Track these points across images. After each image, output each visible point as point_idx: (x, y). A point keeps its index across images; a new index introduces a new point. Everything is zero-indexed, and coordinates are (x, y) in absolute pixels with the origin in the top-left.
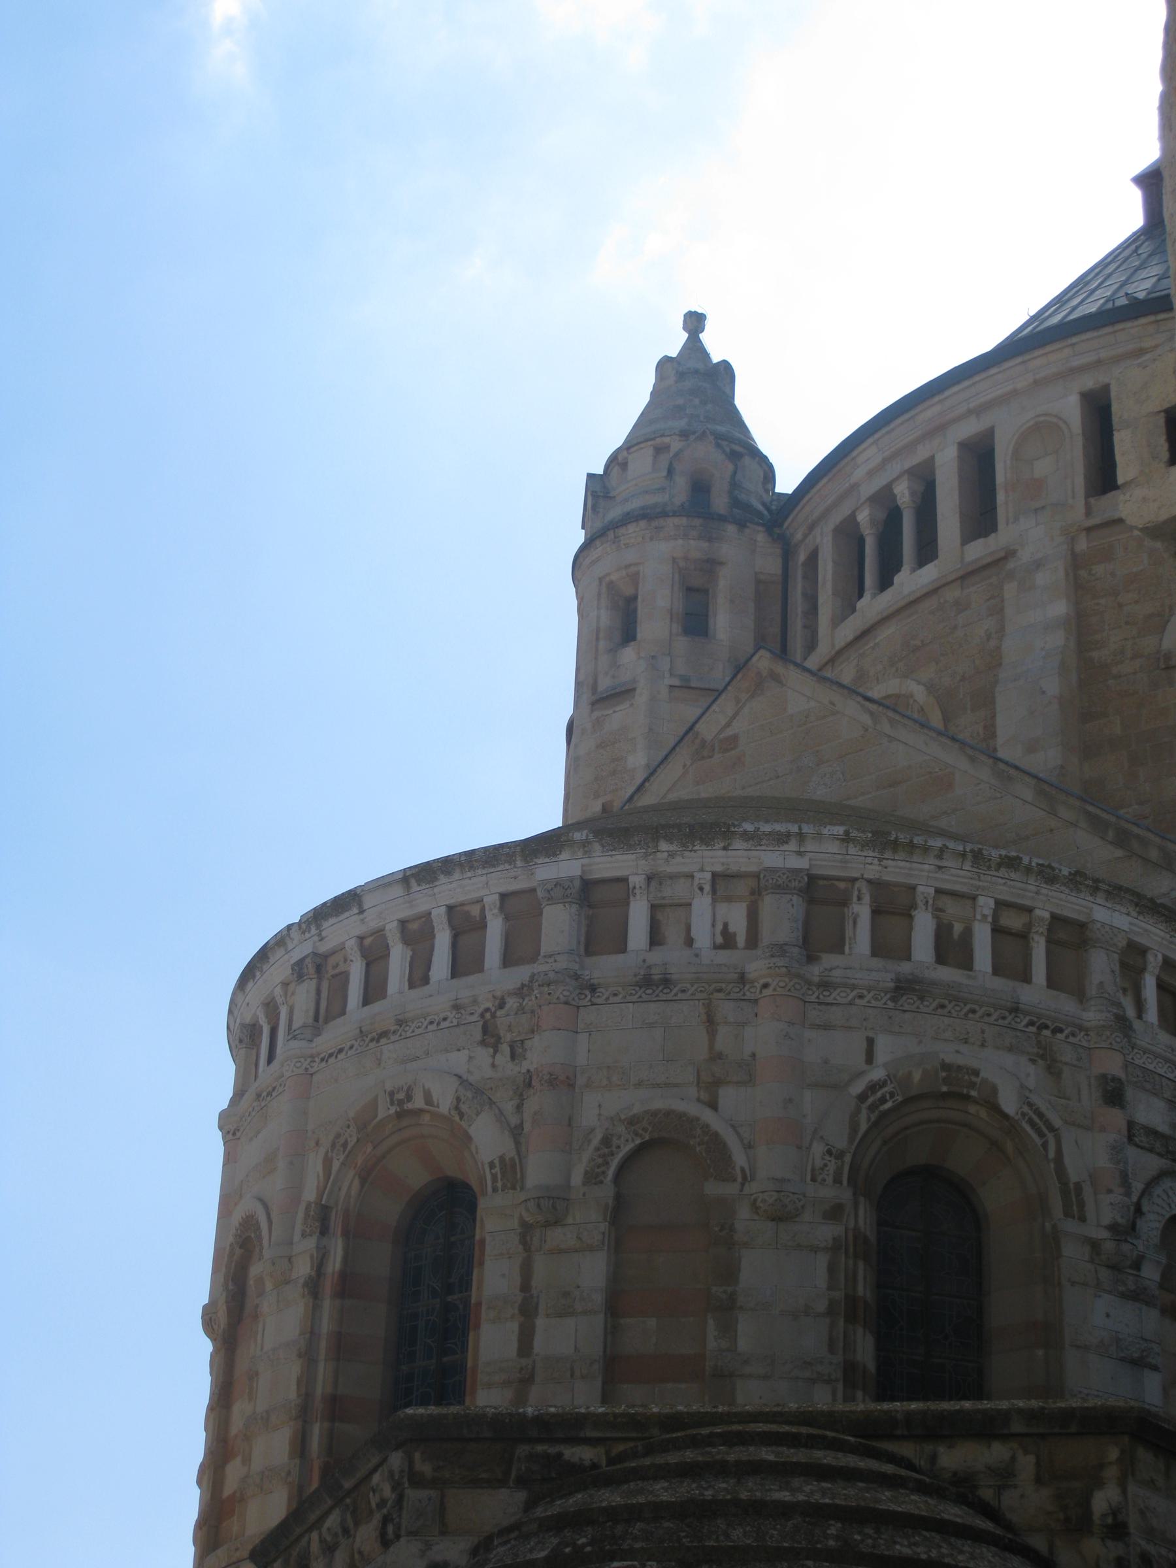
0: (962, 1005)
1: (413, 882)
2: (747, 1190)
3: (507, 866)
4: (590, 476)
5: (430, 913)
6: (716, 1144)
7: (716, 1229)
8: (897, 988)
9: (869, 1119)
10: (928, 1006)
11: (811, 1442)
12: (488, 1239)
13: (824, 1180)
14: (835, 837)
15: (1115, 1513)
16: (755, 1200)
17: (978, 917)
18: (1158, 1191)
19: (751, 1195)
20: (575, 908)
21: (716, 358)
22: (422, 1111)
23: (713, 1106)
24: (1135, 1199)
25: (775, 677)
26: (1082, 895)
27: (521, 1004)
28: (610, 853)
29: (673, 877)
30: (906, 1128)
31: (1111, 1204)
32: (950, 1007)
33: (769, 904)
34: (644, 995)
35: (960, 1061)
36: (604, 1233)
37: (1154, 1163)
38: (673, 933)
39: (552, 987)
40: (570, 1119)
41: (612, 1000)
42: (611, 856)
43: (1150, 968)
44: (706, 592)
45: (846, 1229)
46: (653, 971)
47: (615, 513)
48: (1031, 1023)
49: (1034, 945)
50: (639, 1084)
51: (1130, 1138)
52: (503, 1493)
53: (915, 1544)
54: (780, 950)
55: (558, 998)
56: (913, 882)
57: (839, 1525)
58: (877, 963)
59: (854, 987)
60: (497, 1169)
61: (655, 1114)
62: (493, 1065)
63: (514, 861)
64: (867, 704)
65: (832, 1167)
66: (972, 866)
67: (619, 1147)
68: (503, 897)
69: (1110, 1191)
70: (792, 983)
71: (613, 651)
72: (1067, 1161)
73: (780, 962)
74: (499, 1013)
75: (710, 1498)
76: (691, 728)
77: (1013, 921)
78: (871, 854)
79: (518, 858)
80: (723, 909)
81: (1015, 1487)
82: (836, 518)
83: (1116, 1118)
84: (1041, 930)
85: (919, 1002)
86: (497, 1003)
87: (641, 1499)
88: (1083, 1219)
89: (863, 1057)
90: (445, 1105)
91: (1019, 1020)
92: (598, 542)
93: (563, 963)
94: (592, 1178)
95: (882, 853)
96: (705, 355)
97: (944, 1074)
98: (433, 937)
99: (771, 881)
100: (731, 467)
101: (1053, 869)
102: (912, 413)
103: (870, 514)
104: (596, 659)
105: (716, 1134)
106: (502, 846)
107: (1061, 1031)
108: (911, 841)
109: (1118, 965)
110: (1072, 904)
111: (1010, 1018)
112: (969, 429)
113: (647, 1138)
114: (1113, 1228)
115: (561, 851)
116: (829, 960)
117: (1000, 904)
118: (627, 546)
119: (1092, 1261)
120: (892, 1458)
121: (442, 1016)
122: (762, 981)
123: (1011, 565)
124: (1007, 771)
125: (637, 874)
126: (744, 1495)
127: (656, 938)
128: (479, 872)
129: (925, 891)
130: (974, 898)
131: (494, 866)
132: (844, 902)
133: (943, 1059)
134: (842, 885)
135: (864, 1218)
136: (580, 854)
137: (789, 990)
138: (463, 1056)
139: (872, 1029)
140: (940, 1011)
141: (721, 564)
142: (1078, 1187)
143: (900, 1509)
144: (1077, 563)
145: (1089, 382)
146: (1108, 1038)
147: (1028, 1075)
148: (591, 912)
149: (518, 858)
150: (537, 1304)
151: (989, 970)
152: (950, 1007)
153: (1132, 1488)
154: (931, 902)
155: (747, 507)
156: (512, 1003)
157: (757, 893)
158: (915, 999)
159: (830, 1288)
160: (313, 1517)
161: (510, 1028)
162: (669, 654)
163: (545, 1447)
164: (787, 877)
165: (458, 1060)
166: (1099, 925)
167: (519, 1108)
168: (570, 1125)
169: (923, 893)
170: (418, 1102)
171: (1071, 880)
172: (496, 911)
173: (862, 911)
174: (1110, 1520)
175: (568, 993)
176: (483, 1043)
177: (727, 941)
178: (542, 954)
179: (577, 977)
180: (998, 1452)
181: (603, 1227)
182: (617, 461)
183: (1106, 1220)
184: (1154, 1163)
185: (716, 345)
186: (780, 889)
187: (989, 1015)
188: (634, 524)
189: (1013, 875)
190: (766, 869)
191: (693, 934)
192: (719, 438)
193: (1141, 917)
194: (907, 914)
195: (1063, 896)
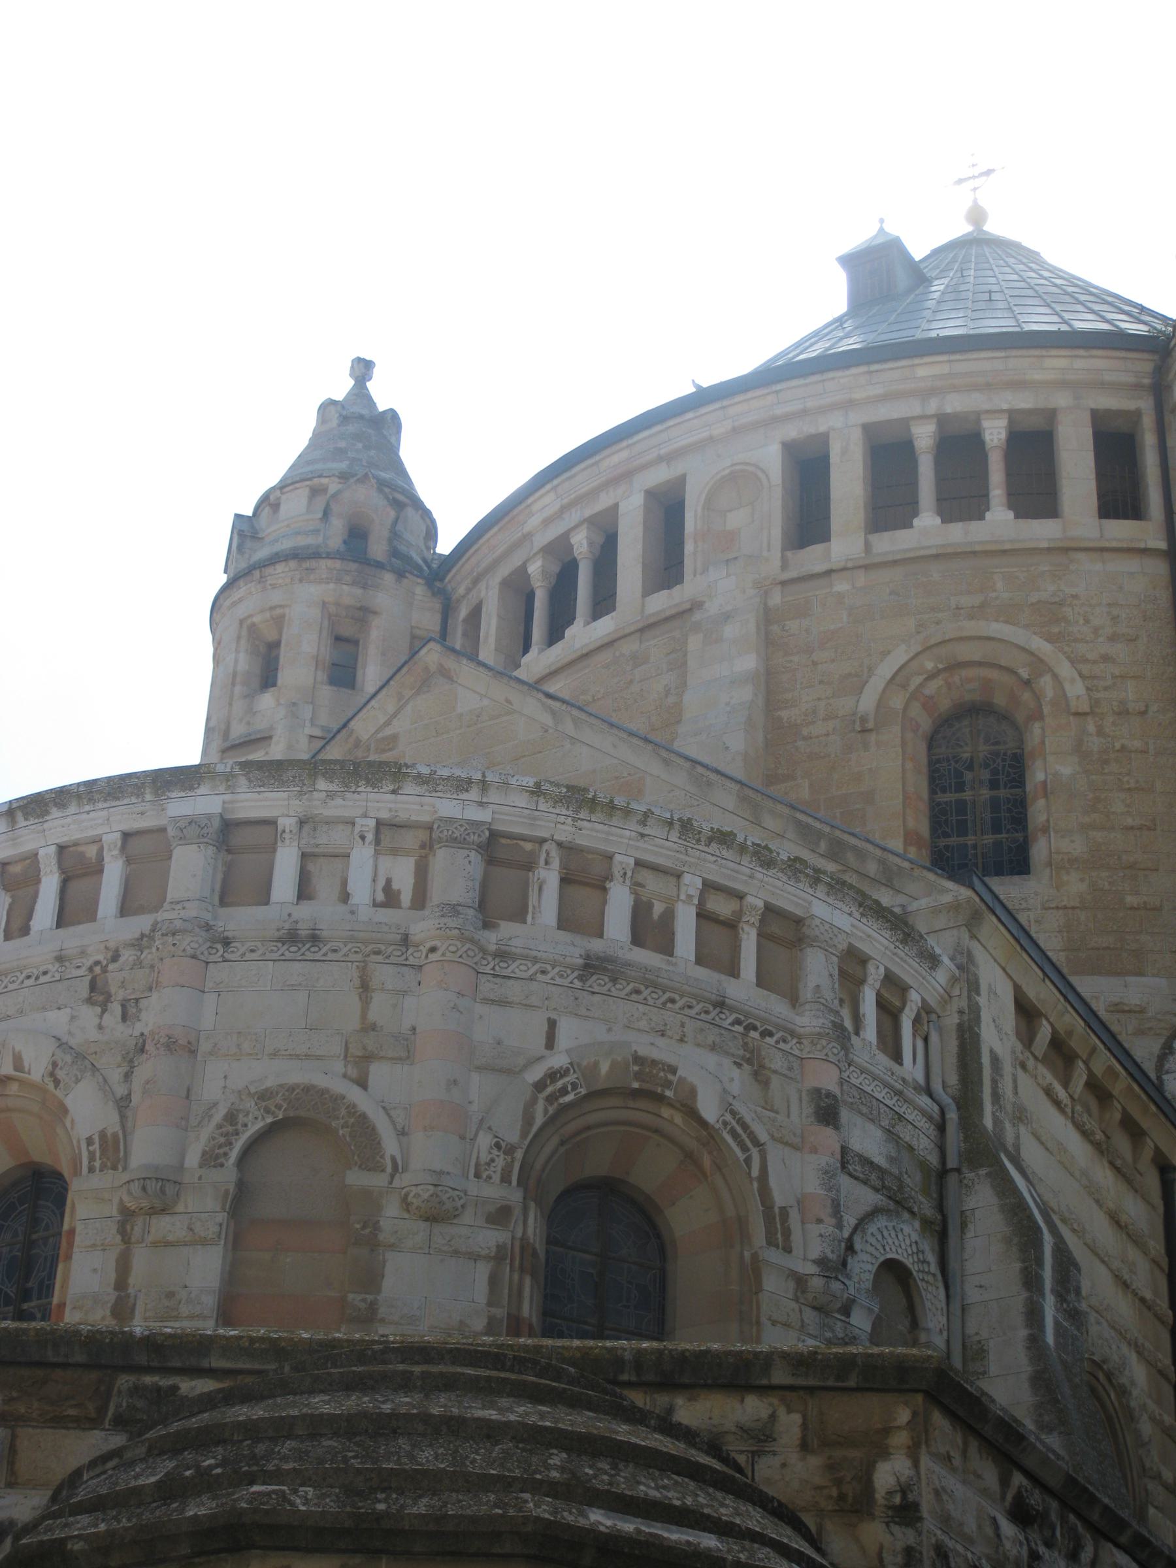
0: (660, 993)
1: (19, 816)
2: (397, 1183)
3: (134, 800)
4: (238, 517)
5: (37, 854)
6: (363, 1127)
7: (358, 1226)
8: (586, 966)
9: (546, 1111)
10: (620, 990)
12: (79, 1228)
13: (490, 1177)
14: (524, 789)
15: (904, 1490)
16: (407, 1195)
17: (683, 897)
18: (872, 1228)
19: (403, 1188)
20: (211, 850)
21: (382, 407)
22: (9, 1078)
23: (363, 1084)
24: (846, 1234)
25: (444, 672)
26: (801, 886)
27: (138, 958)
28: (258, 789)
29: (330, 822)
30: (588, 1128)
31: (821, 1235)
32: (646, 993)
33: (441, 859)
34: (287, 953)
35: (655, 1054)
36: (221, 1225)
37: (867, 1198)
38: (325, 886)
39: (178, 937)
40: (188, 1090)
41: (249, 956)
42: (259, 792)
43: (870, 980)
44: (356, 643)
45: (513, 1238)
46: (299, 926)
47: (263, 553)
48: (738, 1022)
49: (744, 936)
50: (275, 1054)
51: (844, 1165)
52: (97, 1434)
53: (664, 1487)
54: (454, 909)
55: (184, 950)
56: (611, 849)
57: (564, 1455)
58: (563, 936)
59: (535, 960)
60: (96, 1146)
61: (292, 1089)
62: (100, 1027)
63: (142, 794)
64: (550, 702)
65: (500, 1162)
66: (680, 838)
67: (246, 1125)
68: (126, 836)
69: (819, 1221)
70: (465, 949)
71: (250, 696)
72: (773, 1182)
73: (452, 922)
74: (111, 967)
75: (388, 1411)
76: (345, 726)
77: (722, 907)
78: (564, 812)
79: (148, 791)
80: (386, 863)
81: (775, 1453)
82: (504, 571)
83: (828, 1138)
84: (753, 919)
85: (610, 984)
86: (110, 954)
88: (788, 1250)
89: (543, 1041)
90: (37, 1071)
91: (723, 1016)
92: (241, 582)
93: (192, 911)
94: (211, 1159)
95: (577, 812)
97: (636, 1068)
98: (38, 881)
99: (445, 833)
100: (393, 514)
101: (771, 851)
102: (597, 458)
103: (543, 566)
104: (230, 704)
105: (364, 1116)
106: (130, 775)
107: (771, 1034)
108: (612, 802)
109: (837, 970)
111: (713, 1014)
112: (659, 476)
113: (281, 1117)
114: (822, 1262)
115: (199, 784)
116: (507, 930)
117: (709, 886)
118: (274, 586)
119: (796, 1300)
121: (42, 969)
122: (428, 945)
123: (697, 616)
125: (288, 816)
126: (435, 1411)
127: (304, 892)
128: (100, 805)
129: (623, 861)
130: (679, 876)
131: (118, 799)
132: (529, 865)
133: (636, 1051)
134: (528, 846)
135: (533, 1227)
136: (222, 789)
137: (460, 957)
138: (63, 1015)
139: (555, 1009)
140: (634, 997)
141: (375, 613)
142: (784, 1211)
143: (643, 1443)
144: (768, 618)
145: (792, 432)
146: (824, 1047)
147: (732, 1080)
148: (230, 857)
149: (148, 791)
150: (135, 1305)
151: (693, 958)
152: (646, 993)
153: (925, 1461)
154: (629, 874)
155: (407, 559)
156: (127, 956)
157: (428, 847)
158: (607, 979)
159: (490, 1304)
161: (123, 986)
162: (312, 703)
163: (156, 1378)
164: (466, 829)
165: (58, 1020)
166: (817, 922)
167: (128, 1076)
168: (187, 1097)
169: (621, 863)
171: (790, 866)
172: (116, 852)
173: (550, 877)
174: (897, 1500)
175: (196, 946)
176: (90, 1001)
177: (390, 898)
178: (168, 900)
179: (208, 927)
180: (753, 1408)
181: (222, 1217)
182: (269, 502)
183: (815, 1254)
184: (867, 1198)
185: (383, 396)
186: (456, 842)
187: (690, 1007)
188: (283, 564)
189: (725, 853)
190: (441, 819)
191: (351, 888)
192: (382, 485)
193: (864, 920)
194: (601, 887)
195: (779, 884)
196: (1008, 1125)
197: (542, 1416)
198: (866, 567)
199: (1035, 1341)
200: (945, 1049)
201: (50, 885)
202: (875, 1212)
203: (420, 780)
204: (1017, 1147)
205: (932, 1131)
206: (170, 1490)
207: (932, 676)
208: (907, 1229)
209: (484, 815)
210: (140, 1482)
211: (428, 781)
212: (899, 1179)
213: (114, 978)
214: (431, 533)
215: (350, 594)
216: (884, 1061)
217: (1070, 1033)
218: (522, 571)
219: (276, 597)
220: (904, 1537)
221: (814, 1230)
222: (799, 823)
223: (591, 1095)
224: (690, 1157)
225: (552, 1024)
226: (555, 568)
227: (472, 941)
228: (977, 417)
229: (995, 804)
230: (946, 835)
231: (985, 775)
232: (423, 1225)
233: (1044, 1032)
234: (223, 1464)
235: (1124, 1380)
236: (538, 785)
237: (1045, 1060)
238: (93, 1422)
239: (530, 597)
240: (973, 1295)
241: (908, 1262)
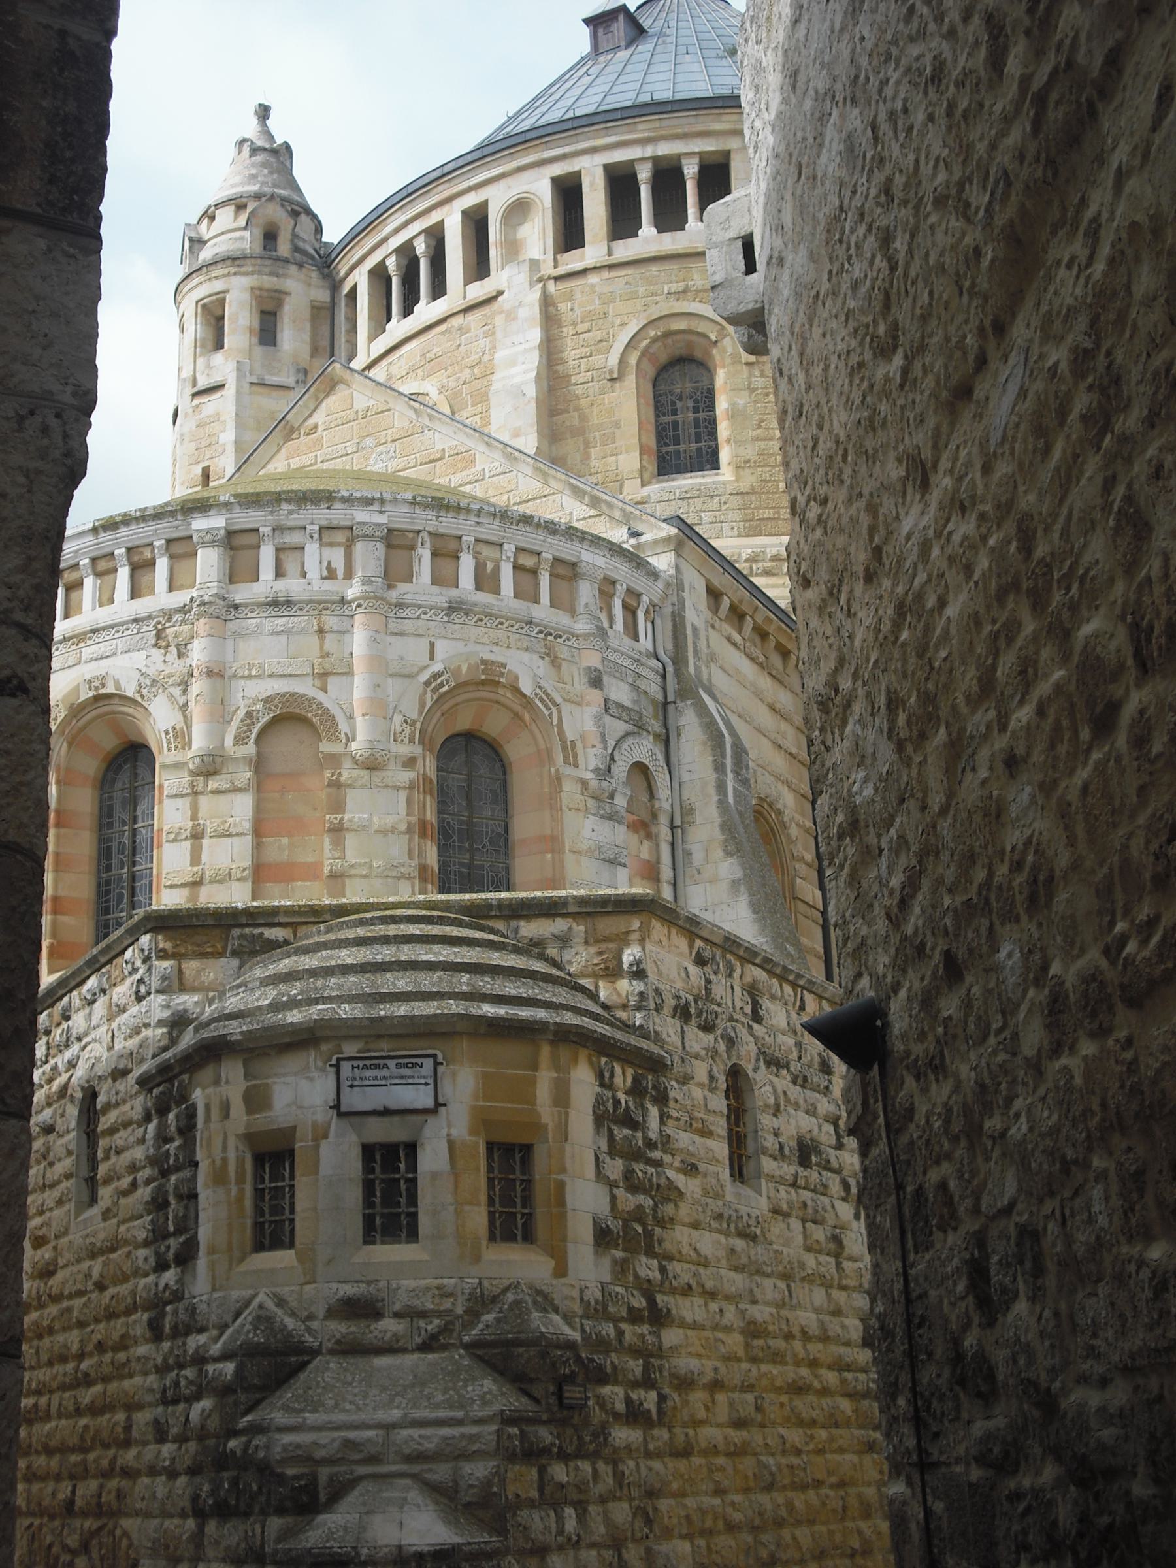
11: (441, 921)
12: (166, 784)
15: (638, 962)
18: (624, 746)
21: (279, 140)
23: (324, 690)
33: (359, 547)
35: (492, 657)
37: (621, 727)
38: (291, 566)
44: (274, 314)
47: (206, 254)
48: (541, 632)
50: (271, 676)
52: (223, 961)
58: (436, 589)
59: (420, 607)
61: (283, 695)
65: (408, 731)
68: (169, 541)
72: (565, 726)
77: (528, 561)
83: (595, 696)
87: (333, 963)
88: (576, 766)
94: (240, 740)
96: (270, 137)
98: (116, 570)
110: (568, 550)
114: (596, 770)
116: (402, 587)
117: (519, 550)
120: (492, 931)
124: (511, 454)
127: (279, 573)
129: (468, 539)
130: (501, 545)
132: (412, 548)
134: (411, 535)
135: (429, 766)
138: (143, 653)
144: (547, 302)
145: (558, 169)
153: (649, 946)
155: (304, 252)
156: (176, 617)
160: (73, 983)
167: (185, 691)
170: (110, 689)
173: (425, 553)
176: (156, 645)
177: (331, 574)
179: (224, 599)
180: (559, 925)
182: (209, 216)
183: (592, 767)
184: (621, 727)
186: (368, 537)
192: (284, 200)
196: (704, 668)
197: (455, 954)
198: (611, 267)
199: (722, 803)
200: (665, 628)
201: (124, 574)
202: (627, 734)
203: (344, 500)
204: (710, 680)
205: (659, 680)
206: (275, 1007)
207: (655, 340)
208: (645, 743)
209: (383, 519)
210: (260, 1003)
211: (349, 501)
212: (640, 713)
213: (170, 631)
214: (319, 230)
215: (269, 282)
216: (627, 641)
217: (741, 602)
218: (381, 266)
219: (218, 286)
220: (639, 986)
221: (591, 752)
222: (571, 485)
223: (458, 686)
224: (517, 715)
225: (432, 645)
226: (405, 262)
227: (382, 599)
228: (679, 157)
229: (697, 422)
230: (667, 445)
231: (691, 404)
232: (366, 772)
233: (726, 603)
234: (302, 992)
235: (779, 806)
236: (414, 498)
237: (727, 619)
238: (220, 955)
239: (389, 280)
240: (686, 777)
241: (646, 762)
